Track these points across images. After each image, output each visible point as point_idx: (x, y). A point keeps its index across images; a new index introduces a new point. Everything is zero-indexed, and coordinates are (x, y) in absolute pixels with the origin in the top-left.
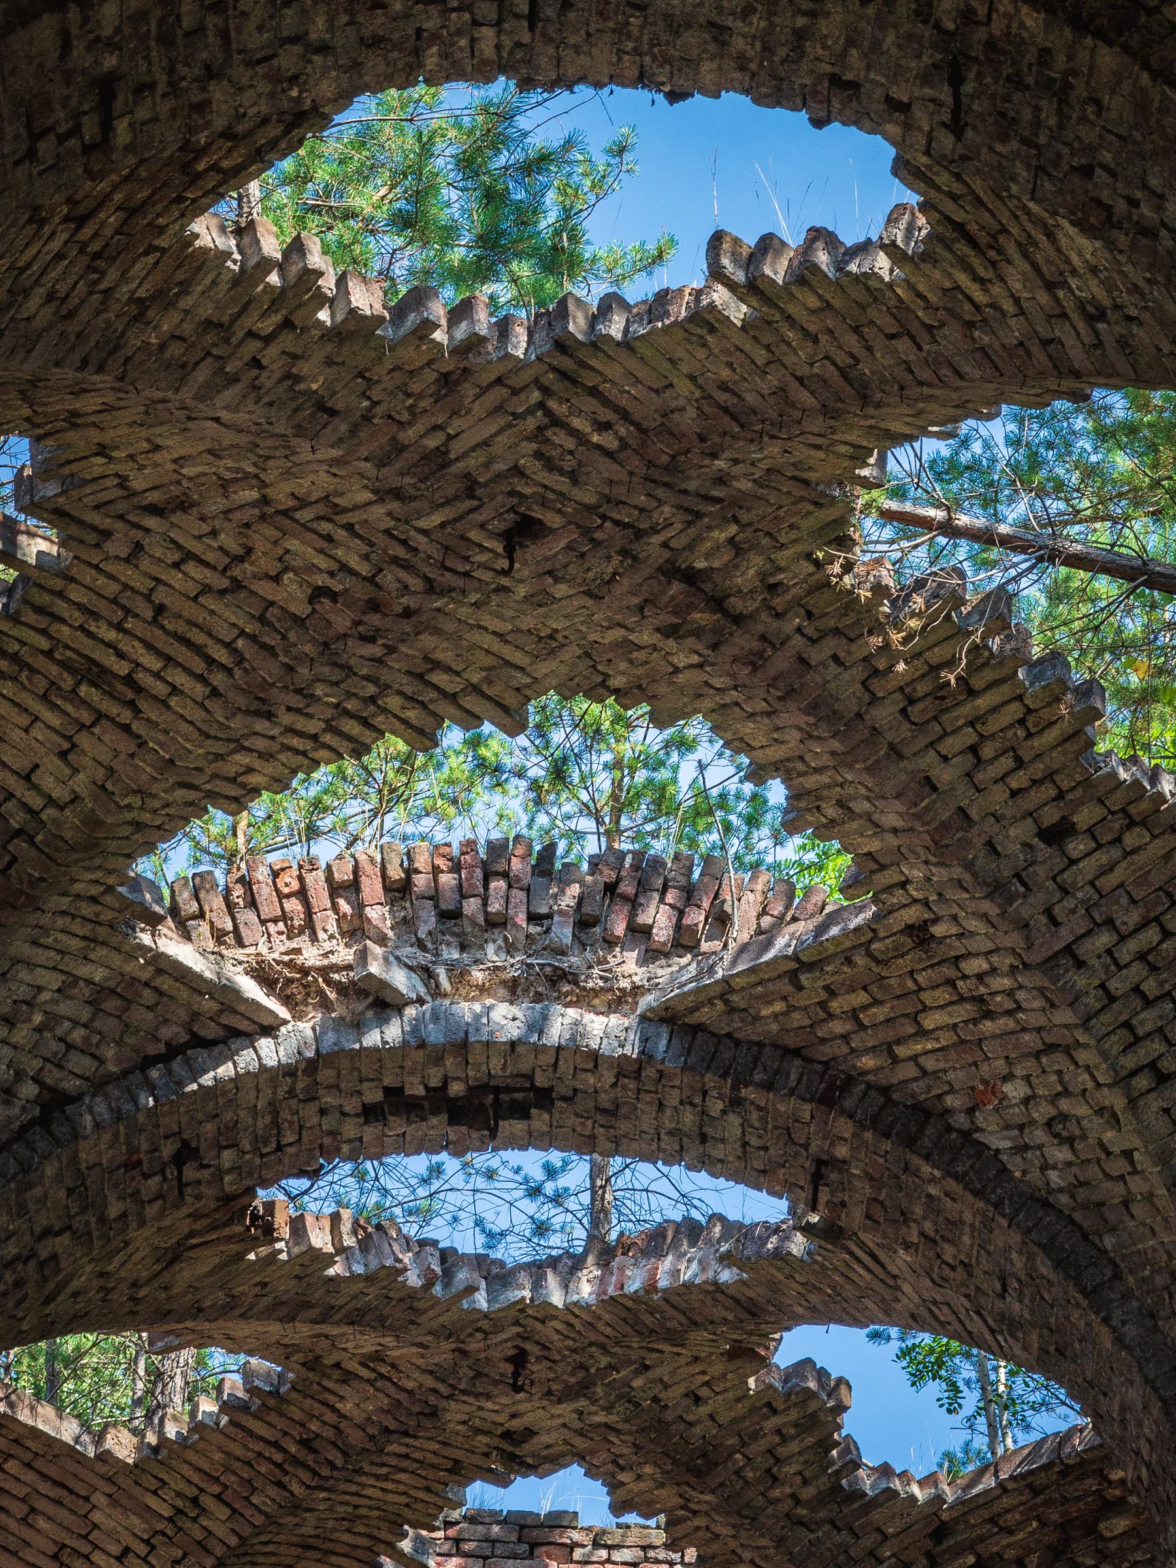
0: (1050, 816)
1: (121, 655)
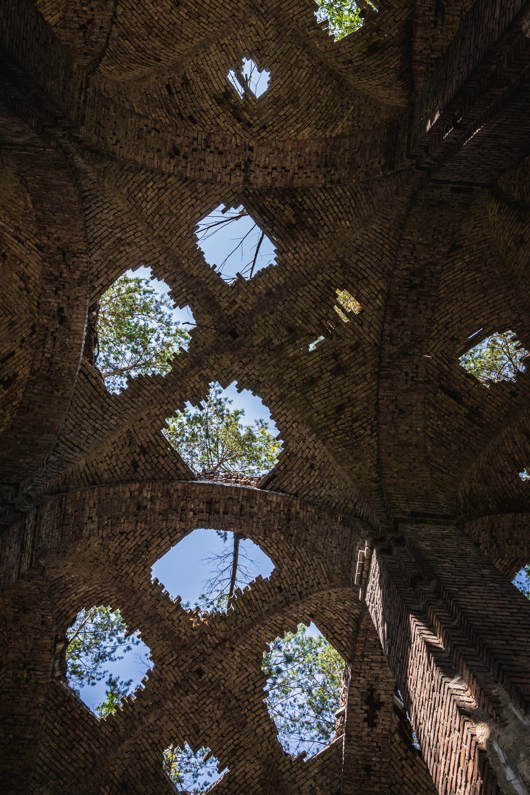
0: (277, 590)
1: (230, 746)
